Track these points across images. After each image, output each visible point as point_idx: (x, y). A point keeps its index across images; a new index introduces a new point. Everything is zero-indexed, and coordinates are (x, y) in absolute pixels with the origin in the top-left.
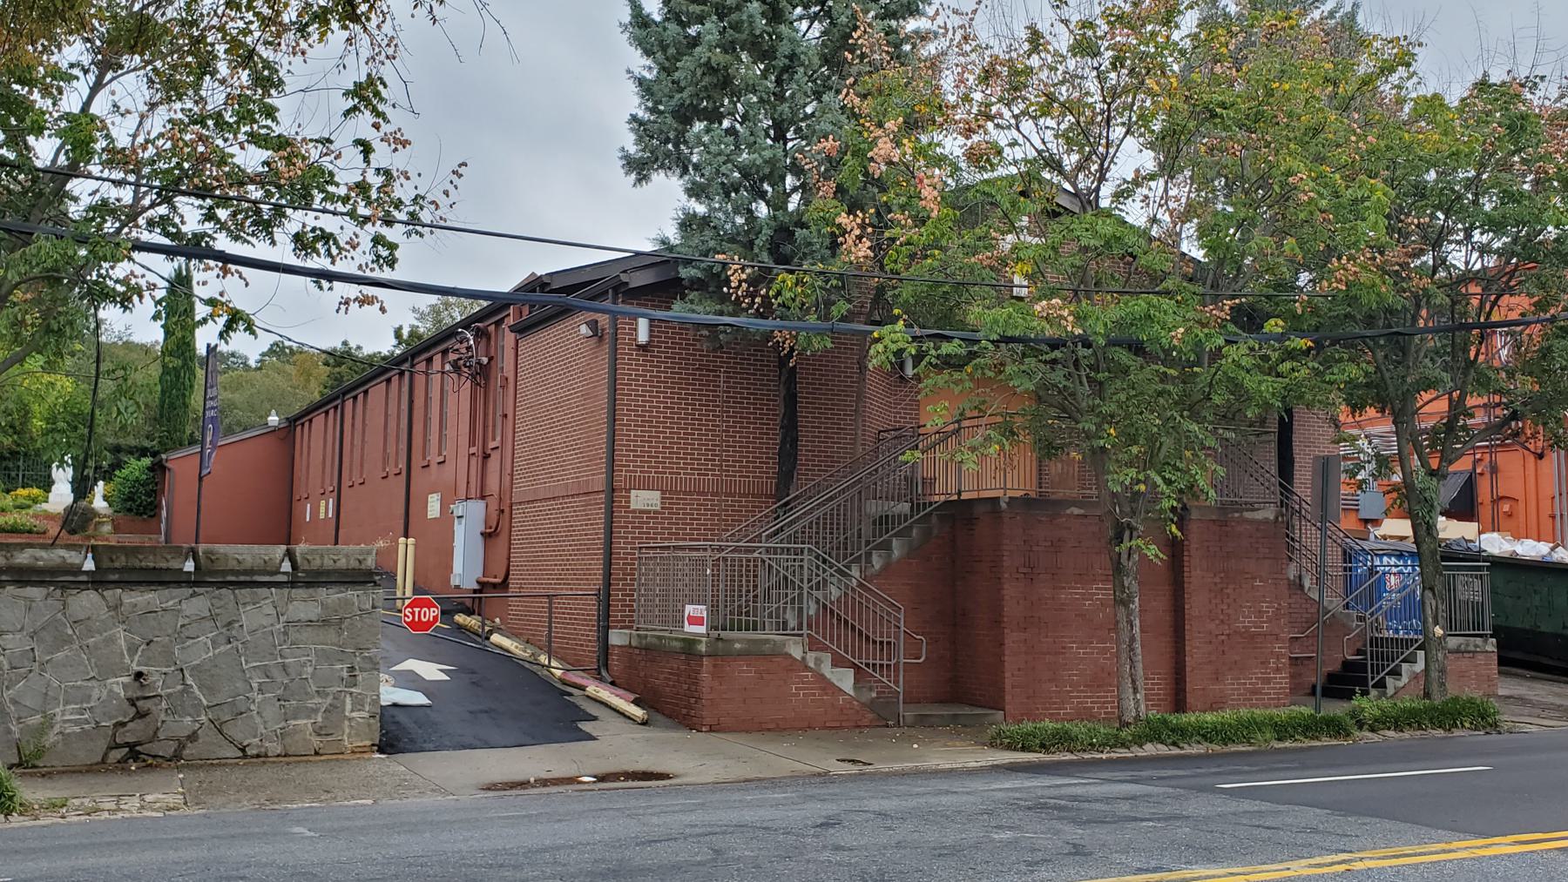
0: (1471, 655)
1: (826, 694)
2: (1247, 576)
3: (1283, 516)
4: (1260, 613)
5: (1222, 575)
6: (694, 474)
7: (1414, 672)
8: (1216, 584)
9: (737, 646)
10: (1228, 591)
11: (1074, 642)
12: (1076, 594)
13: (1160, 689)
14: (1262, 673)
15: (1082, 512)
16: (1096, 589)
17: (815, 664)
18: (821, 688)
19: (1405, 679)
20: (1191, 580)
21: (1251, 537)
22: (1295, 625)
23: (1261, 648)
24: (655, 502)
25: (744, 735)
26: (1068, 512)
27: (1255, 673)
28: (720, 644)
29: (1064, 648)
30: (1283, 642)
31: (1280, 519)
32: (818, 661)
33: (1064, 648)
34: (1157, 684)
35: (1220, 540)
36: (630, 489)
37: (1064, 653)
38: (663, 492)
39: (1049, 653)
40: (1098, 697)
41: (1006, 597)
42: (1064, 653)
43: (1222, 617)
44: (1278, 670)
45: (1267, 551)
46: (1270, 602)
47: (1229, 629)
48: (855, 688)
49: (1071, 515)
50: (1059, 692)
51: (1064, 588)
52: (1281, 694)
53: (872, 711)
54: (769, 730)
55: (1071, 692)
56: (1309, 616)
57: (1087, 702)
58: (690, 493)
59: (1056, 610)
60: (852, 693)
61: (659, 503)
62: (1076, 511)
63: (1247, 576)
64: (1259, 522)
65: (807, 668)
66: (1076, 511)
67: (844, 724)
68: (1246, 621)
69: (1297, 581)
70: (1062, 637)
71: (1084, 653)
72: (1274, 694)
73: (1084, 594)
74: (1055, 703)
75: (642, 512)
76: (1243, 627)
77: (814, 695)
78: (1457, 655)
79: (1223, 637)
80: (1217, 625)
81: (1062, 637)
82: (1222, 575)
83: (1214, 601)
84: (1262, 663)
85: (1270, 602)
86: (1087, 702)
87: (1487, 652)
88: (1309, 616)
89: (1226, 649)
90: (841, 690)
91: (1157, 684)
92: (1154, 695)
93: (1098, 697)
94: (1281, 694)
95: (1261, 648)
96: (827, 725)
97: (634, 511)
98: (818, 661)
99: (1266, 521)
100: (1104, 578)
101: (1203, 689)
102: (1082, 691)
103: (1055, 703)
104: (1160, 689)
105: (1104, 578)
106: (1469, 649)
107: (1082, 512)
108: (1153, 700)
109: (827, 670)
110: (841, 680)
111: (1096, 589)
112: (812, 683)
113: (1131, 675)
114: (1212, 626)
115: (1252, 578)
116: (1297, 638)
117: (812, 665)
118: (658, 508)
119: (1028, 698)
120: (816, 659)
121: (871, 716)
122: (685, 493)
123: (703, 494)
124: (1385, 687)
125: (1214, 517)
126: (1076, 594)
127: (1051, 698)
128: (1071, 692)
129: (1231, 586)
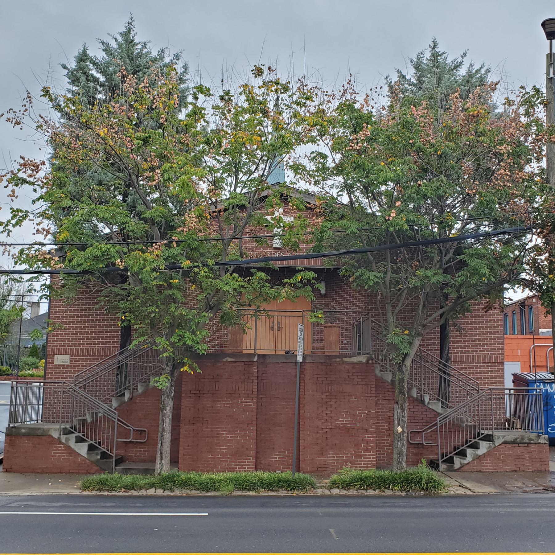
0: (526, 445)
1: (71, 456)
2: (345, 394)
3: (372, 360)
4: (354, 416)
5: (327, 394)
6: (87, 347)
7: (477, 455)
8: (322, 399)
9: (23, 431)
10: (331, 403)
11: (225, 431)
12: (228, 404)
13: (289, 459)
14: (355, 451)
15: (233, 360)
16: (240, 402)
17: (66, 441)
18: (67, 453)
19: (469, 459)
20: (305, 396)
21: (348, 372)
22: (418, 424)
23: (355, 436)
24: (66, 361)
25: (19, 474)
26: (225, 360)
27: (351, 451)
28: (14, 430)
29: (218, 434)
30: (371, 433)
31: (370, 362)
32: (67, 440)
33: (218, 434)
34: (287, 456)
35: (326, 374)
36: (54, 355)
37: (217, 437)
38: (72, 356)
39: (208, 437)
40: (239, 462)
41: (182, 407)
42: (217, 437)
43: (326, 418)
44: (367, 450)
45: (360, 380)
46: (362, 410)
47: (331, 425)
48: (88, 454)
49: (227, 361)
50: (214, 458)
51: (220, 401)
52: (370, 464)
53: (97, 465)
54: (38, 473)
55: (221, 458)
56: (429, 419)
57: (232, 465)
58: (85, 356)
59: (213, 413)
60: (86, 456)
61: (69, 361)
62: (229, 359)
63: (345, 394)
64: (354, 364)
65: (60, 443)
66: (229, 359)
67: (80, 472)
68: (344, 420)
69: (419, 398)
70: (217, 428)
71: (231, 437)
72: (364, 464)
73: (232, 405)
74: (210, 464)
75: (59, 365)
76: (342, 424)
77: (64, 456)
78: (514, 445)
79: (327, 430)
80: (322, 423)
81: (217, 428)
82: (327, 394)
83: (320, 409)
84: (355, 445)
85: (362, 410)
86: (232, 465)
87: (540, 443)
88: (429, 419)
89: (329, 436)
90: (79, 454)
91: (287, 456)
92: (285, 461)
93: (239, 462)
94: (370, 464)
95: (355, 436)
96: (71, 471)
97: (56, 365)
98: (67, 440)
99: (360, 363)
100: (246, 396)
101: (312, 459)
102: (229, 458)
103: (210, 464)
104: (289, 459)
105: (246, 396)
106: (524, 441)
107: (233, 360)
108: (284, 464)
109: (72, 444)
110: (80, 449)
111: (240, 402)
112: (63, 450)
113: (161, 450)
114: (319, 423)
115: (349, 396)
116: (419, 432)
117: (63, 441)
118: (68, 363)
119: (193, 461)
120: (66, 438)
121: (96, 468)
122: (83, 356)
123: (93, 356)
124: (453, 463)
125: (322, 361)
126: (228, 404)
127: (208, 461)
128: (221, 458)
129: (334, 400)
